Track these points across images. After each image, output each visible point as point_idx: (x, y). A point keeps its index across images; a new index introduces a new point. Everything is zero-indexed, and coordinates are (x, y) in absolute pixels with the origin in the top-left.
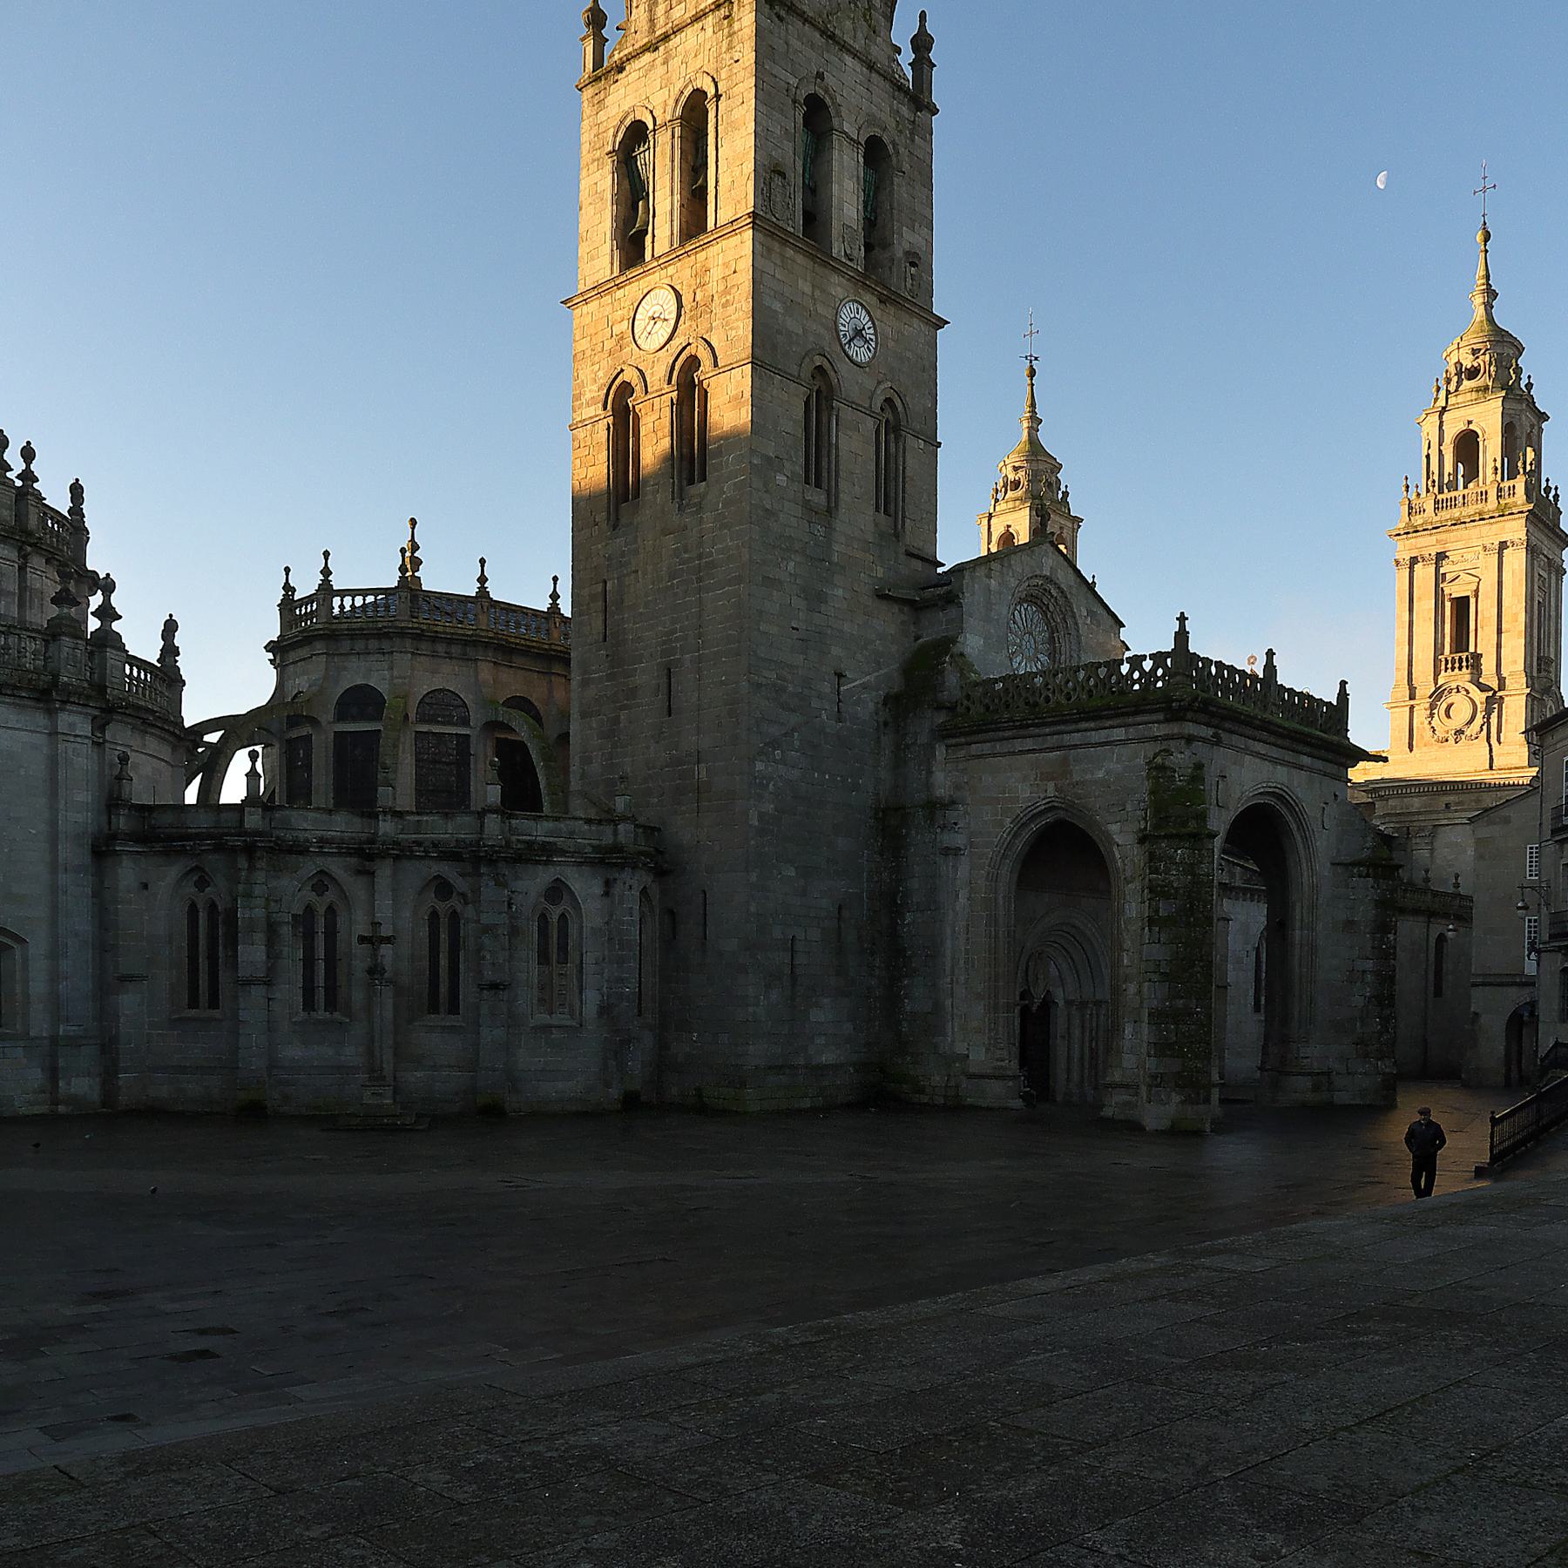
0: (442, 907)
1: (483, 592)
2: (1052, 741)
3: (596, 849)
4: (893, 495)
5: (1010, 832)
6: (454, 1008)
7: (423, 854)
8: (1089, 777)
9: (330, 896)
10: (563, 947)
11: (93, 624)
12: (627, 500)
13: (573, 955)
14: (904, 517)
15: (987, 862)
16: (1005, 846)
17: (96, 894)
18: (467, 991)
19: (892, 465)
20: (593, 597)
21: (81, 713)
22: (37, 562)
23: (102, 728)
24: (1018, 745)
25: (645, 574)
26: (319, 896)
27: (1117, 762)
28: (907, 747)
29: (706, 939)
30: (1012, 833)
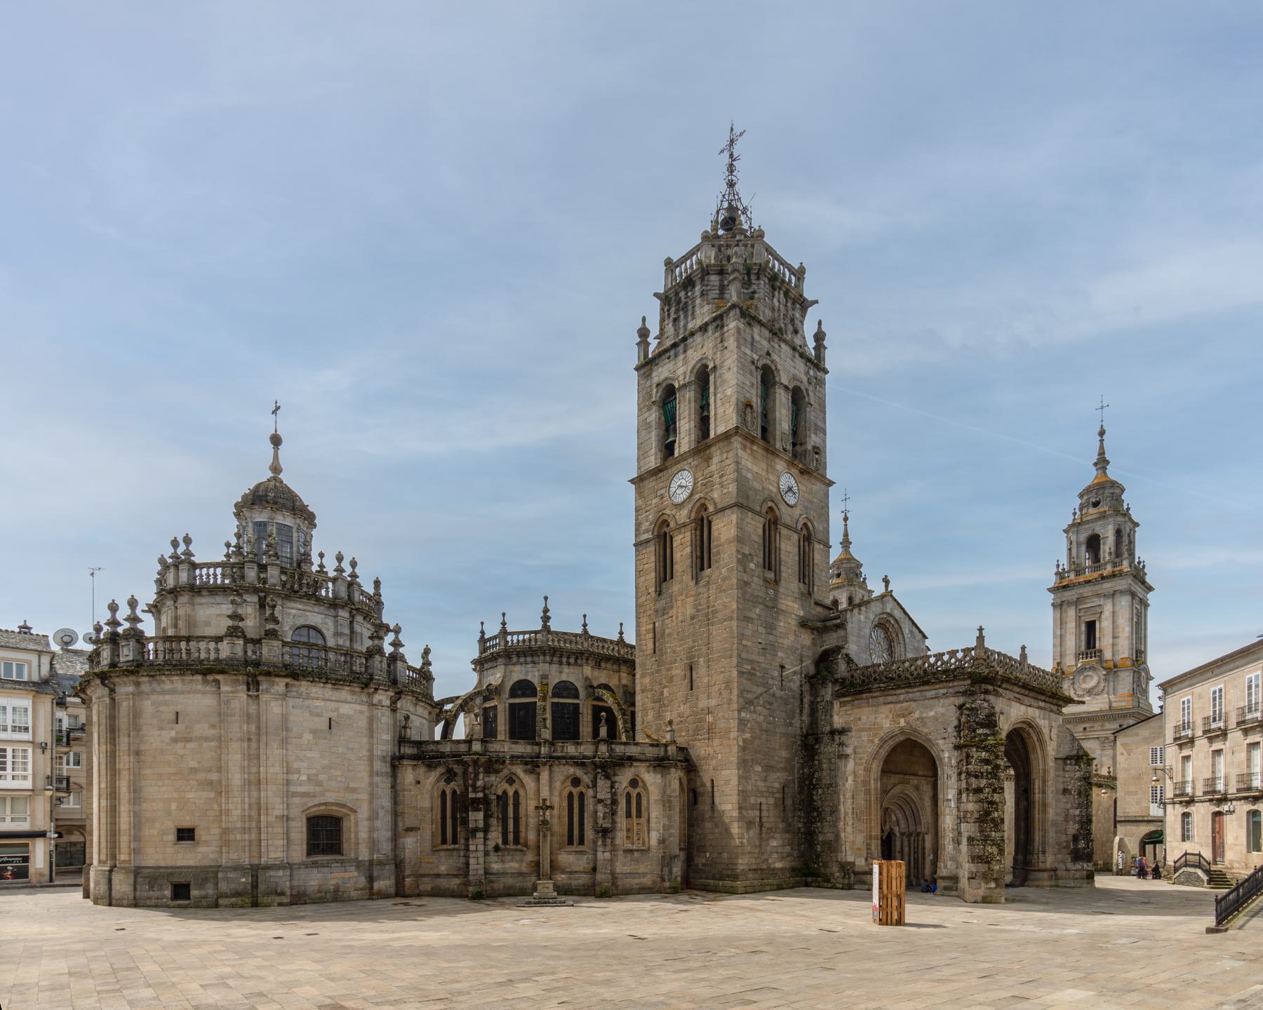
1: (586, 632)
12: (665, 580)
17: (393, 787)
19: (807, 558)
25: (677, 618)
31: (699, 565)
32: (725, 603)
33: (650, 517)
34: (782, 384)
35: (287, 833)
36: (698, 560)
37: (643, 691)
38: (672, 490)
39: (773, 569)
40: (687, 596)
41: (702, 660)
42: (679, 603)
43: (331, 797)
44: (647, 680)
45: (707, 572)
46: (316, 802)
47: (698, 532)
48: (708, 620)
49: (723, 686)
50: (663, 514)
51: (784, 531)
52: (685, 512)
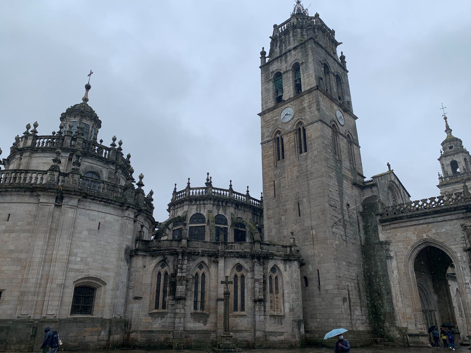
0: (239, 274)
2: (422, 222)
3: (286, 255)
4: (351, 159)
5: (411, 250)
6: (243, 309)
7: (233, 256)
8: (439, 231)
9: (203, 270)
10: (277, 288)
11: (136, 187)
12: (279, 160)
13: (280, 291)
14: (355, 164)
15: (404, 261)
16: (409, 255)
18: (248, 303)
20: (270, 186)
21: (132, 211)
22: (120, 171)
23: (136, 217)
24: (408, 224)
25: (288, 178)
26: (200, 270)
27: (449, 226)
28: (369, 226)
29: (320, 285)
30: (412, 251)
31: (299, 151)
32: (317, 168)
33: (270, 130)
34: (332, 72)
35: (62, 297)
36: (299, 149)
37: (268, 218)
38: (282, 117)
39: (337, 154)
40: (294, 166)
41: (305, 200)
42: (289, 170)
43: (93, 273)
44: (271, 212)
45: (305, 154)
46: (83, 275)
47: (298, 135)
48: (307, 178)
49: (320, 213)
50: (277, 128)
51: (341, 137)
52: (290, 126)
